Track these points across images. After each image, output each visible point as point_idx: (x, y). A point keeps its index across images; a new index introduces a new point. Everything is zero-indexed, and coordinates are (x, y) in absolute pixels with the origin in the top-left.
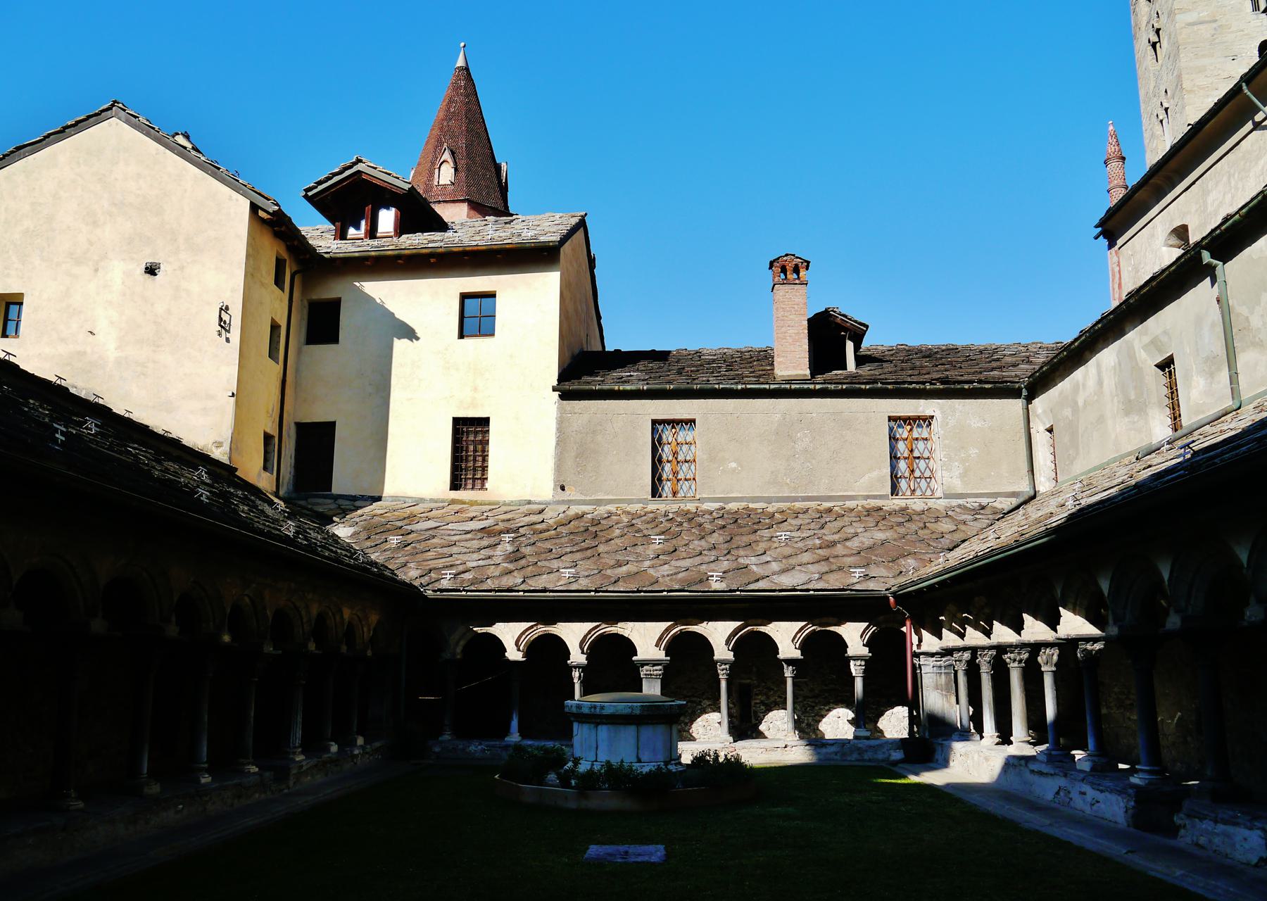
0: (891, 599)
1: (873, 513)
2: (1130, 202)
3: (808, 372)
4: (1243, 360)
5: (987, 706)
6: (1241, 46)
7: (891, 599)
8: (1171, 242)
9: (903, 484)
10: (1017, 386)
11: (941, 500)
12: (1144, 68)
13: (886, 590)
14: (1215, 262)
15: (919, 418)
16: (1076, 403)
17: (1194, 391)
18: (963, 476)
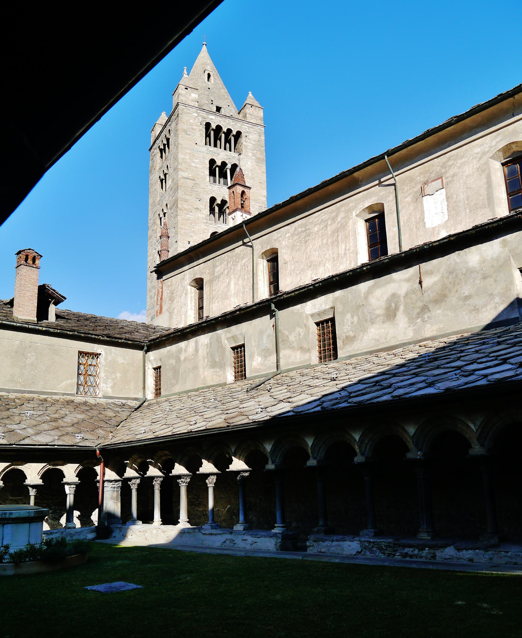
0: (98, 451)
1: (70, 403)
2: (176, 260)
3: (36, 319)
4: (282, 353)
5: (157, 506)
7: (98, 451)
8: (192, 284)
9: (81, 388)
10: (143, 344)
11: (102, 399)
12: (154, 189)
13: (96, 446)
14: (276, 310)
15: (93, 354)
16: (179, 358)
17: (255, 362)
18: (112, 387)
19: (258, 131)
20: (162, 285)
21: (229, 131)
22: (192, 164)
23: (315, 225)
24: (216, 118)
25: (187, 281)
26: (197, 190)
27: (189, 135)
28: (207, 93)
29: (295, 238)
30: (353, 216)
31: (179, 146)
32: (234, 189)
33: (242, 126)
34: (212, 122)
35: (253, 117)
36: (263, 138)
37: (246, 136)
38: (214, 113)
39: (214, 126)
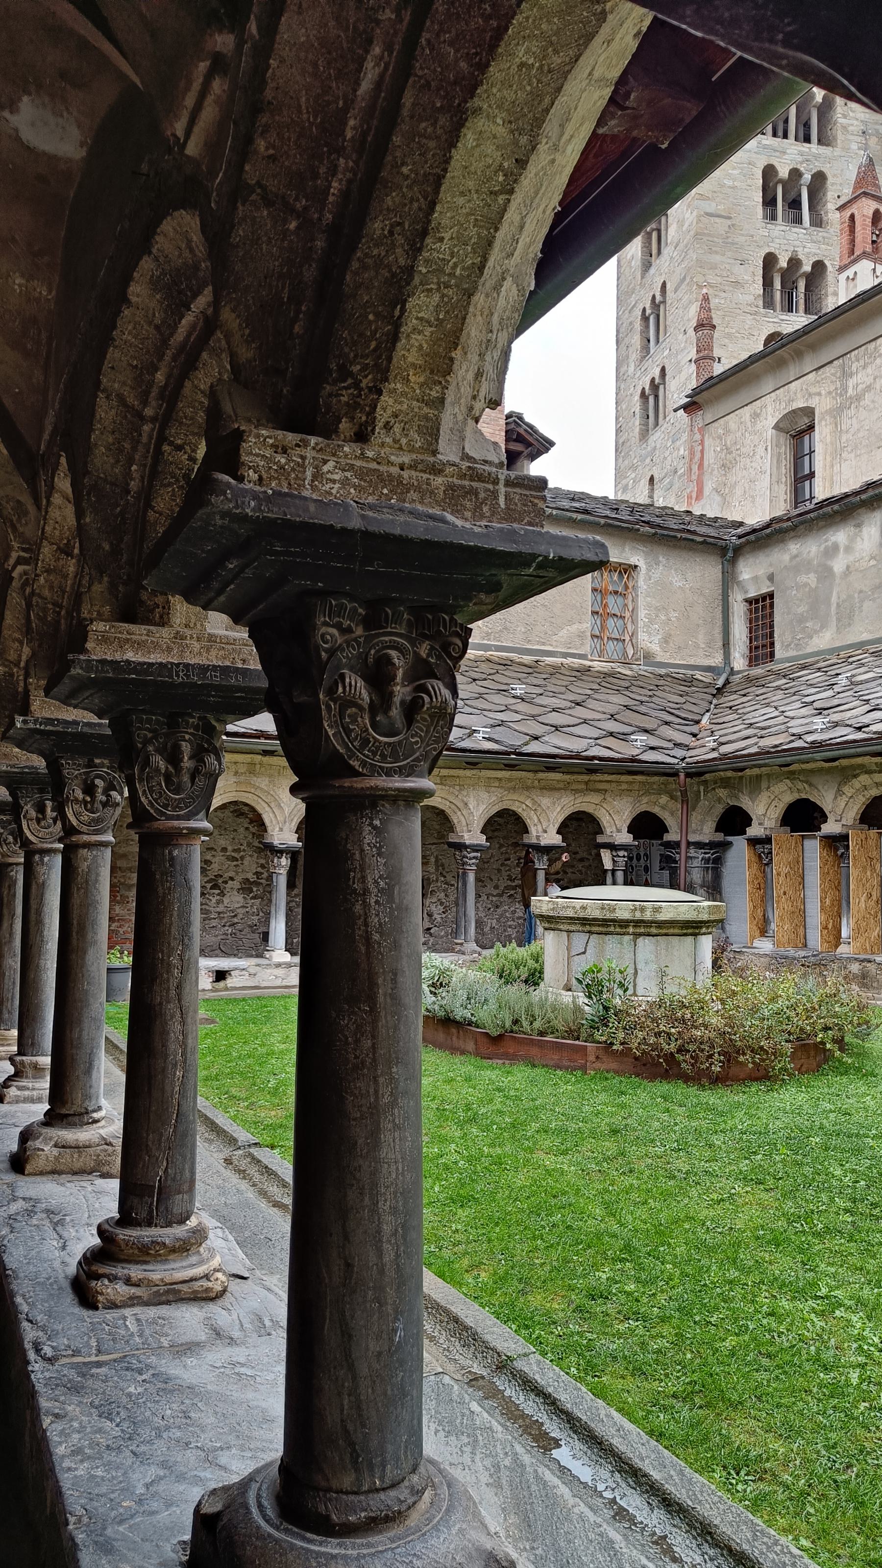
16: (830, 570)
18: (666, 640)
20: (703, 436)
25: (770, 417)
32: (854, 209)
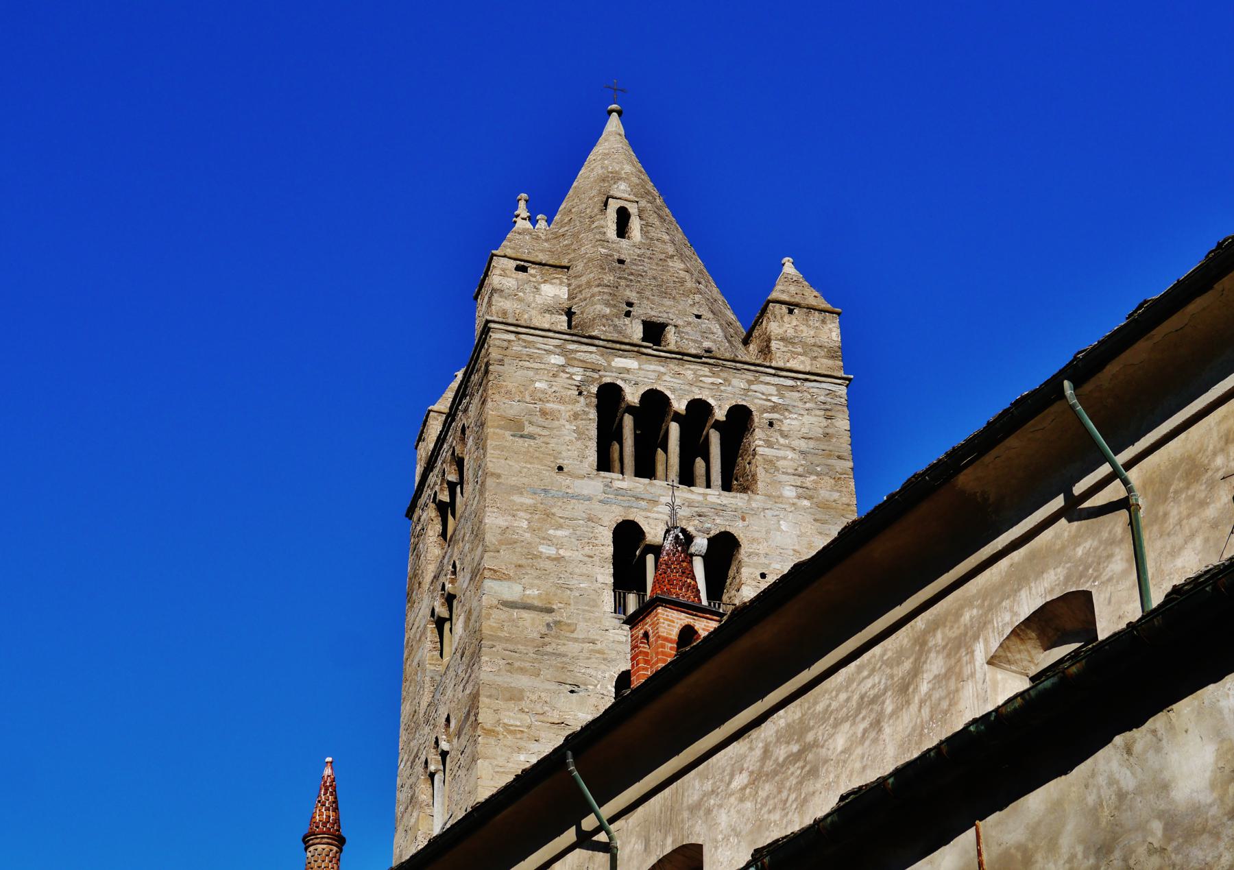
6: (588, 671)
19: (822, 398)
21: (699, 409)
22: (543, 549)
23: (836, 725)
24: (646, 367)
26: (562, 649)
27: (531, 437)
28: (609, 278)
29: (767, 789)
30: (978, 664)
31: (490, 482)
33: (753, 387)
34: (624, 380)
35: (800, 350)
36: (843, 423)
37: (771, 424)
38: (636, 349)
39: (633, 396)
